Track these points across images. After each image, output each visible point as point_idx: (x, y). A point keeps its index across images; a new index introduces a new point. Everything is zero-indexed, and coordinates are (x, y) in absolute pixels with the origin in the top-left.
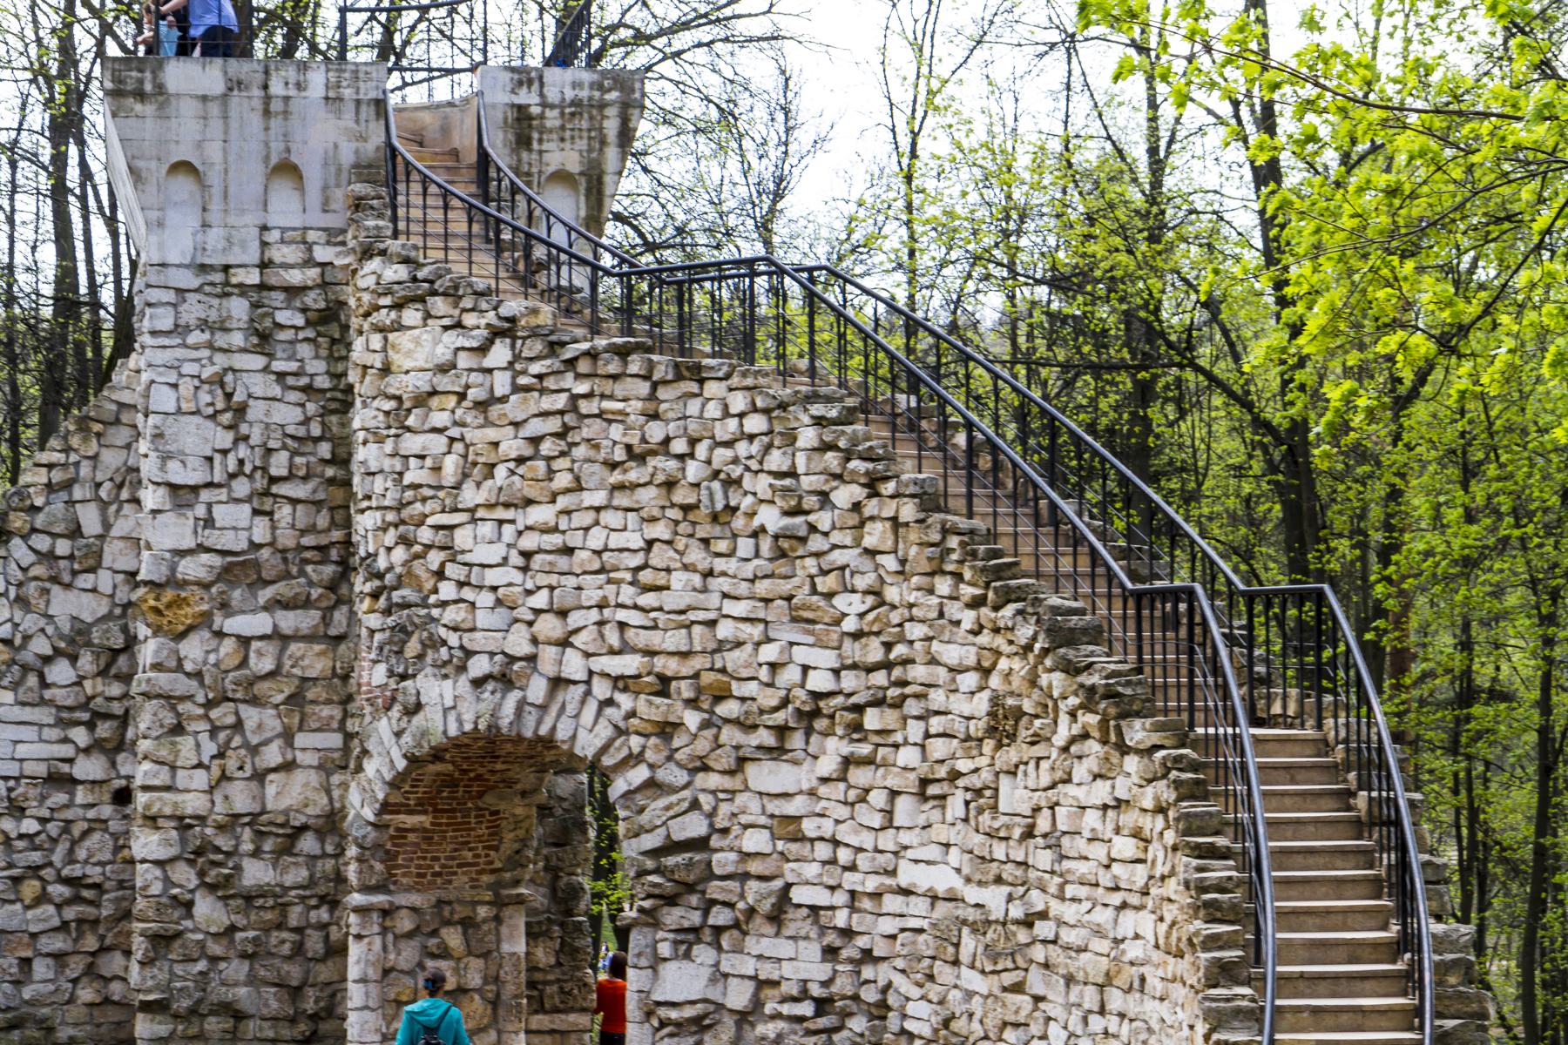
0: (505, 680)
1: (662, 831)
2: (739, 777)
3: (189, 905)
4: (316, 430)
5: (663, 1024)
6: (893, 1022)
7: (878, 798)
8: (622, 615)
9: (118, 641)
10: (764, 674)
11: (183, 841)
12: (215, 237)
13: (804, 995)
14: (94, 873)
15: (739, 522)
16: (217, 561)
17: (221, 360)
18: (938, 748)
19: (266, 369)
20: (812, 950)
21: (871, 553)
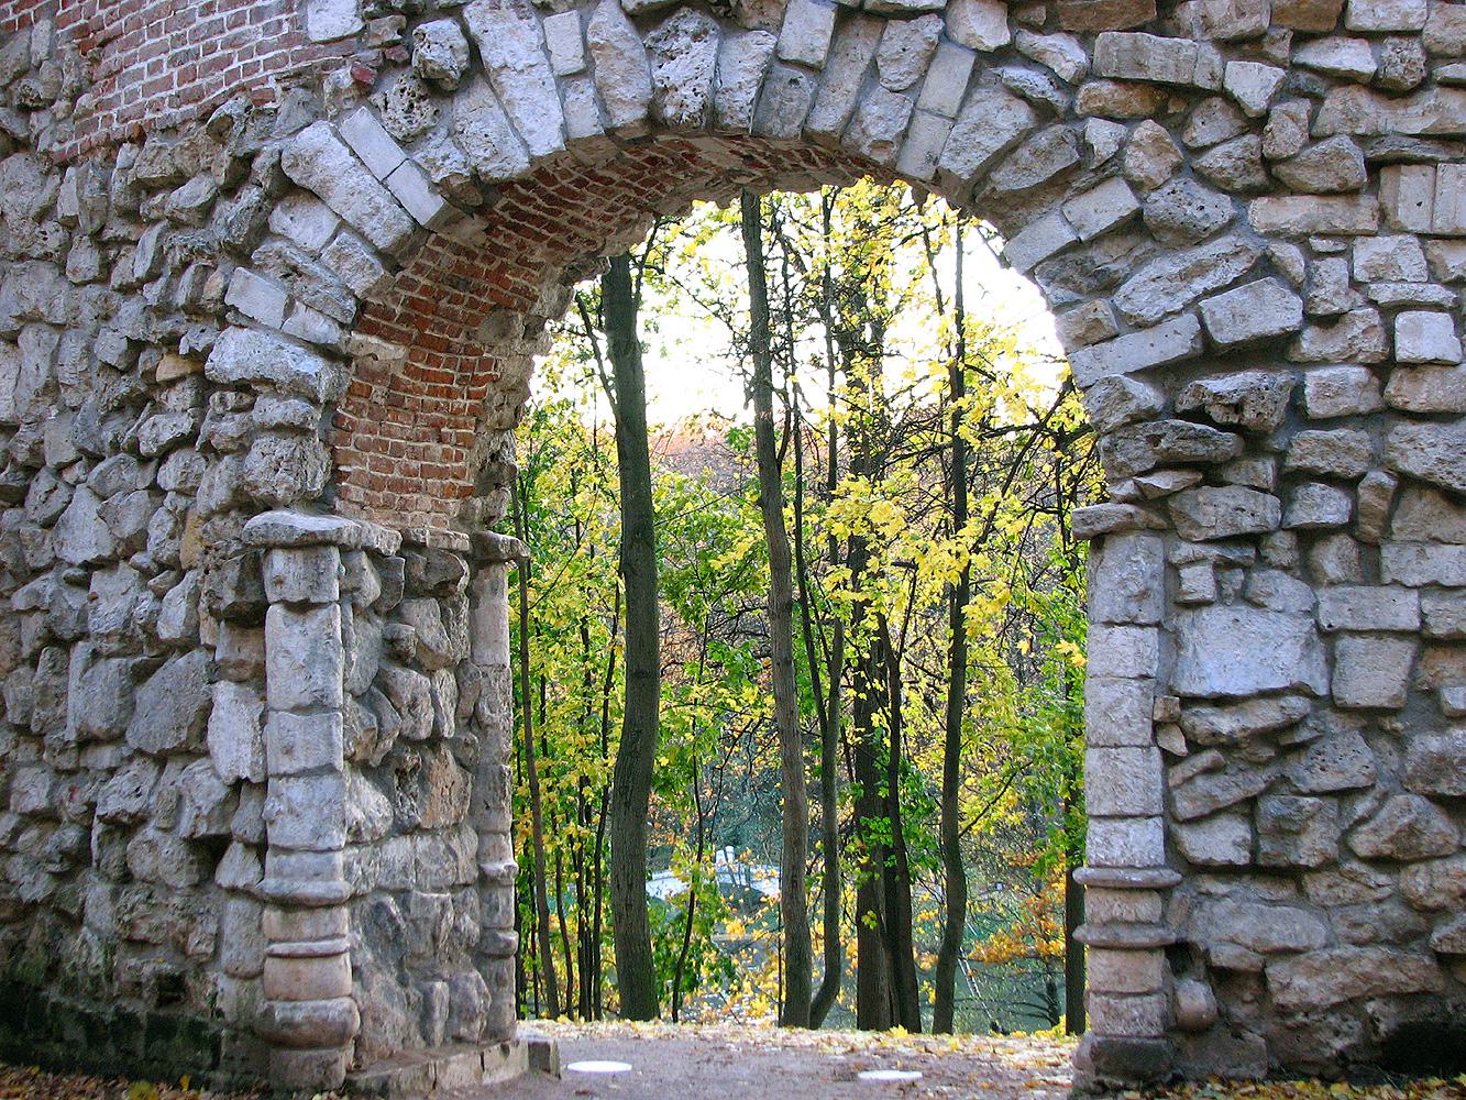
1: (1188, 323)
2: (1367, 203)
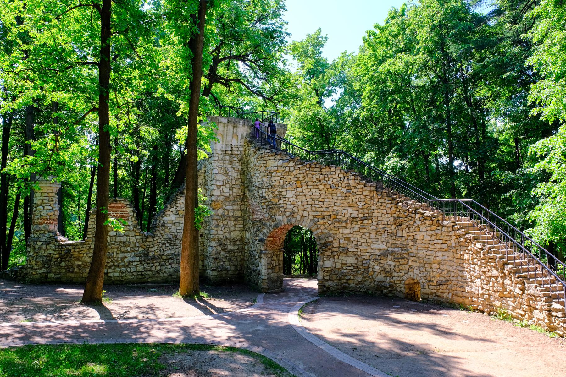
3: (220, 253)
8: (315, 206)
12: (224, 146)
13: (352, 266)
16: (224, 198)
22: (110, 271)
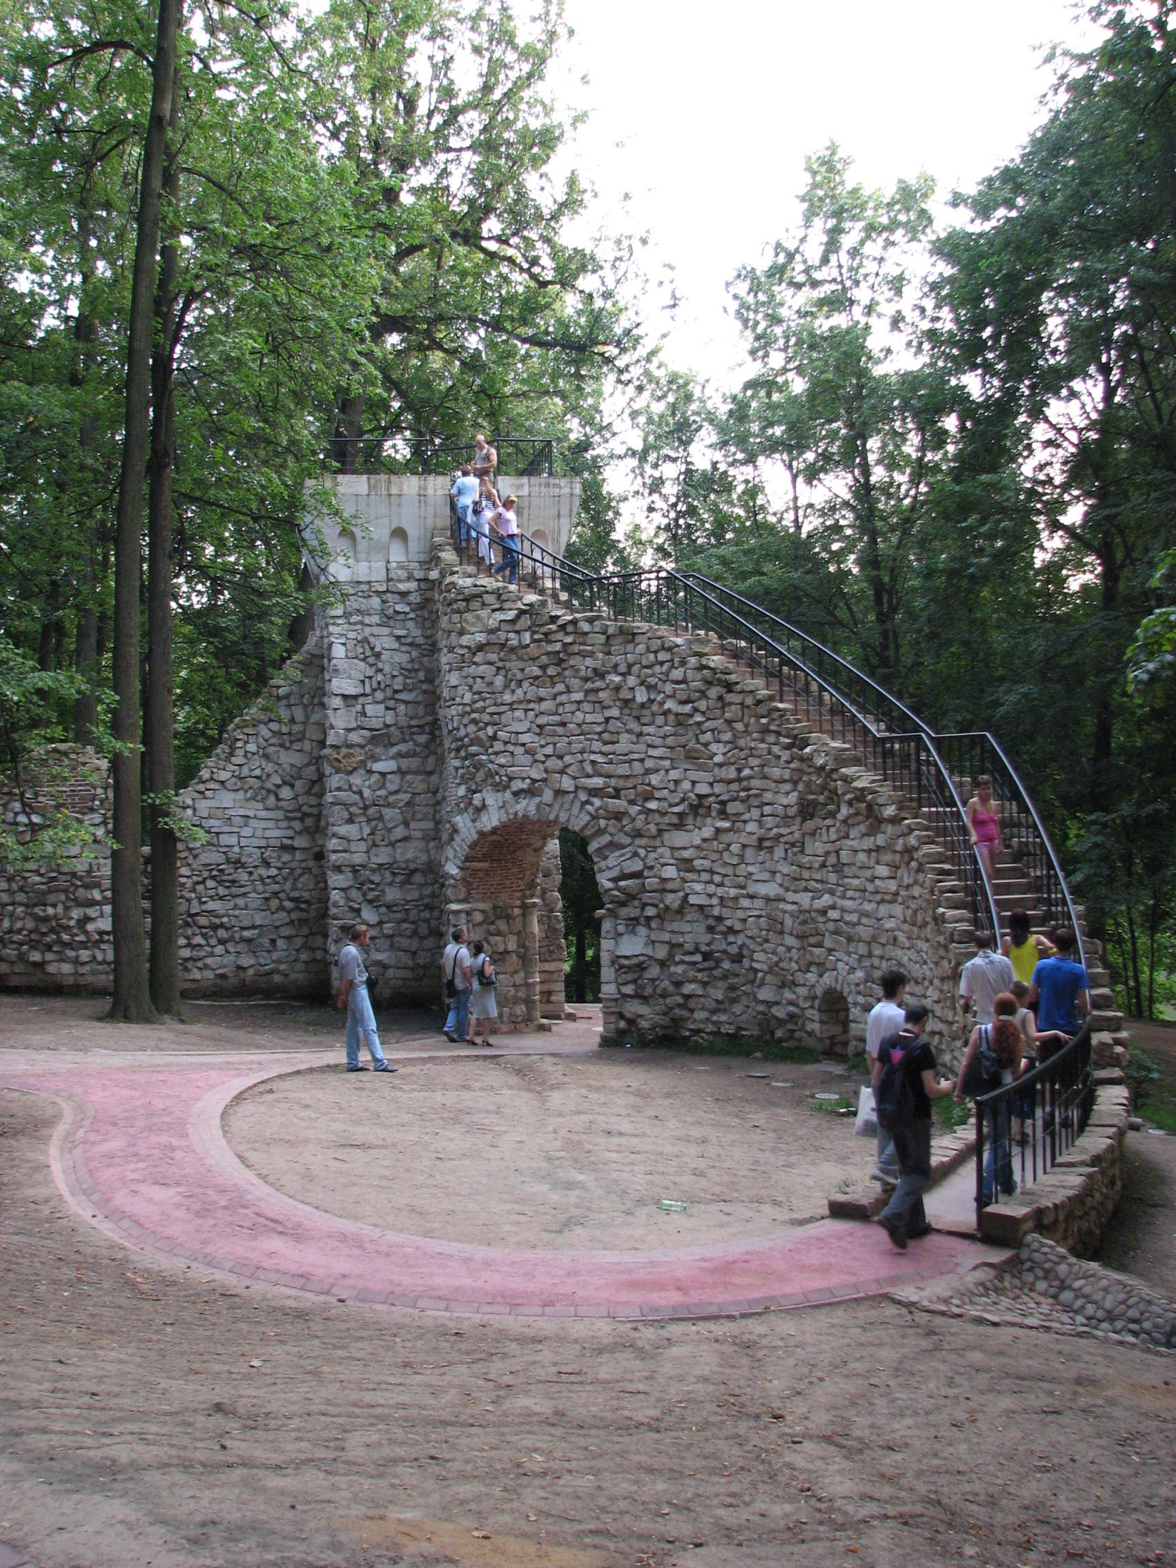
0: (531, 792)
3: (358, 911)
4: (416, 666)
5: (621, 967)
6: (746, 962)
7: (735, 848)
8: (593, 757)
9: (315, 777)
10: (671, 786)
11: (355, 878)
14: (306, 895)
15: (655, 708)
17: (368, 630)
18: (770, 821)
19: (391, 634)
20: (700, 928)
21: (729, 722)
22: (49, 956)
